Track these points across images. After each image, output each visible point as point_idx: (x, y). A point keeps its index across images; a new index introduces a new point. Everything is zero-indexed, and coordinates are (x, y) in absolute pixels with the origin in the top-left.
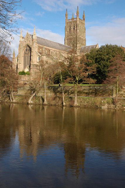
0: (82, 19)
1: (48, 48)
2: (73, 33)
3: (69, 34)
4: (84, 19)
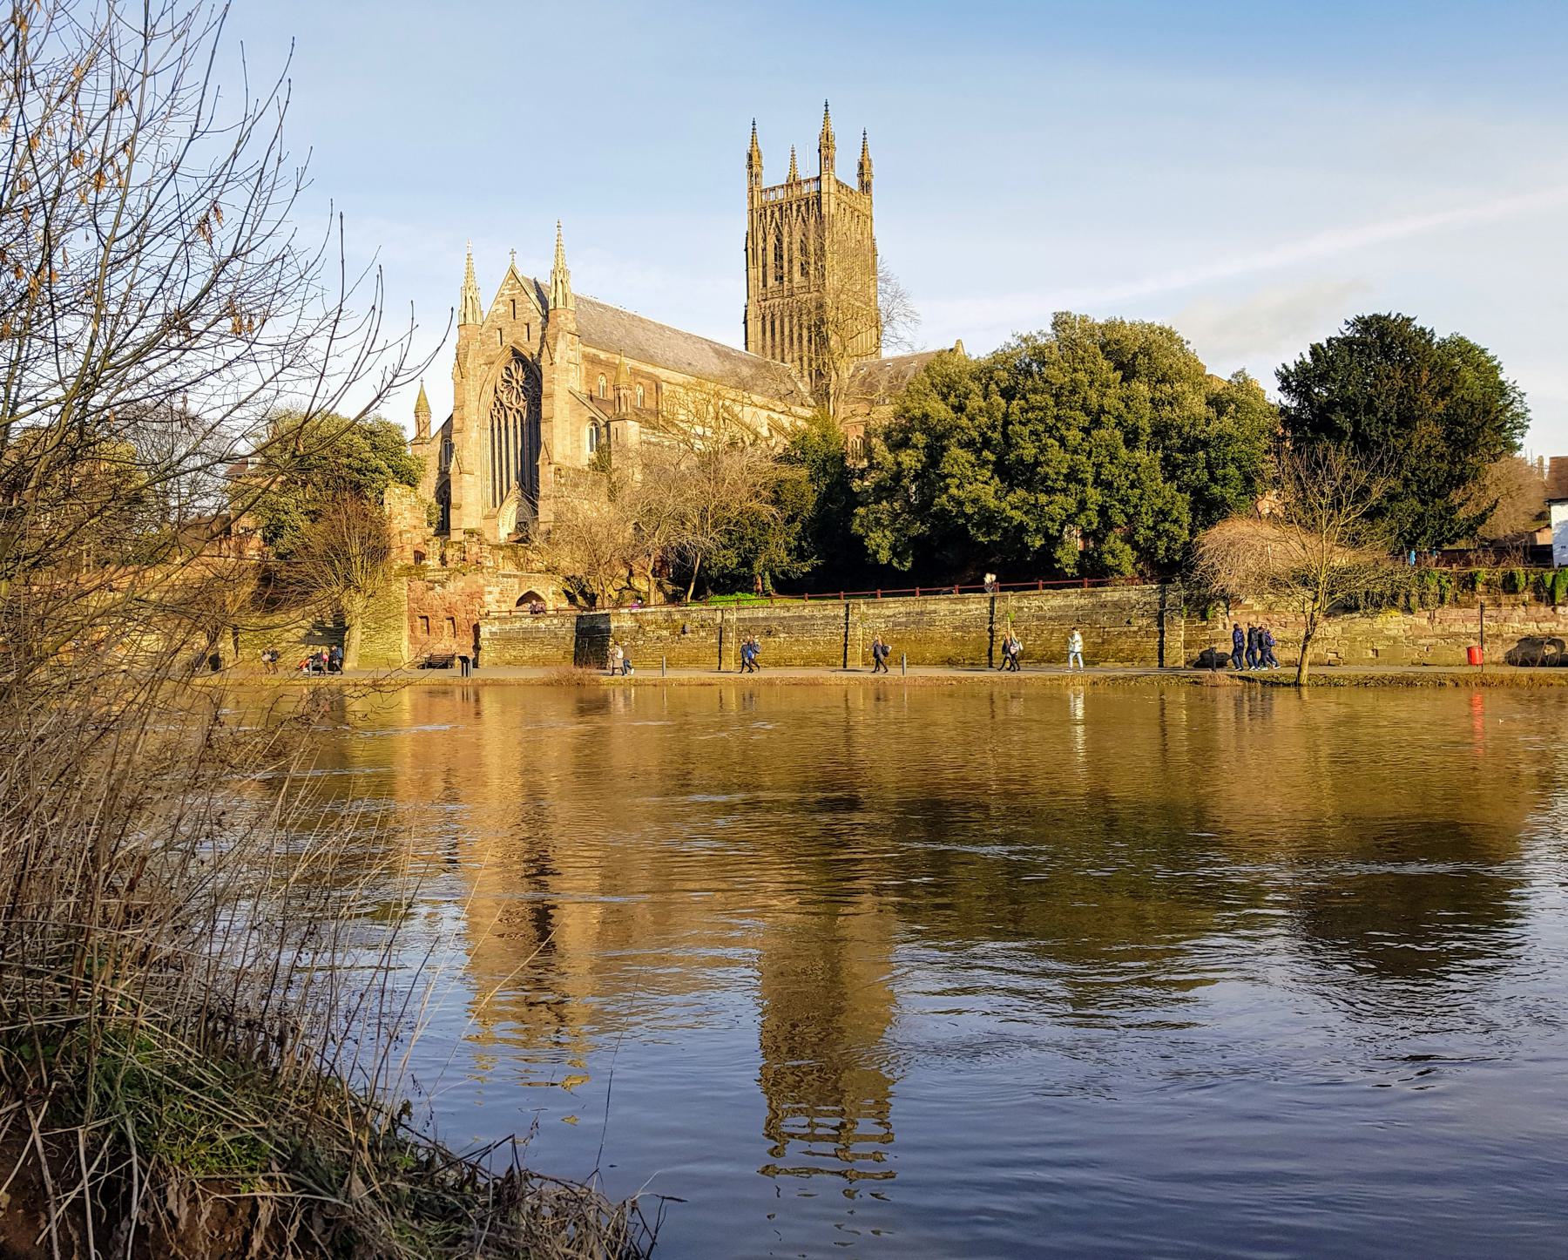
0: (854, 184)
1: (649, 369)
2: (797, 276)
3: (771, 282)
4: (865, 187)
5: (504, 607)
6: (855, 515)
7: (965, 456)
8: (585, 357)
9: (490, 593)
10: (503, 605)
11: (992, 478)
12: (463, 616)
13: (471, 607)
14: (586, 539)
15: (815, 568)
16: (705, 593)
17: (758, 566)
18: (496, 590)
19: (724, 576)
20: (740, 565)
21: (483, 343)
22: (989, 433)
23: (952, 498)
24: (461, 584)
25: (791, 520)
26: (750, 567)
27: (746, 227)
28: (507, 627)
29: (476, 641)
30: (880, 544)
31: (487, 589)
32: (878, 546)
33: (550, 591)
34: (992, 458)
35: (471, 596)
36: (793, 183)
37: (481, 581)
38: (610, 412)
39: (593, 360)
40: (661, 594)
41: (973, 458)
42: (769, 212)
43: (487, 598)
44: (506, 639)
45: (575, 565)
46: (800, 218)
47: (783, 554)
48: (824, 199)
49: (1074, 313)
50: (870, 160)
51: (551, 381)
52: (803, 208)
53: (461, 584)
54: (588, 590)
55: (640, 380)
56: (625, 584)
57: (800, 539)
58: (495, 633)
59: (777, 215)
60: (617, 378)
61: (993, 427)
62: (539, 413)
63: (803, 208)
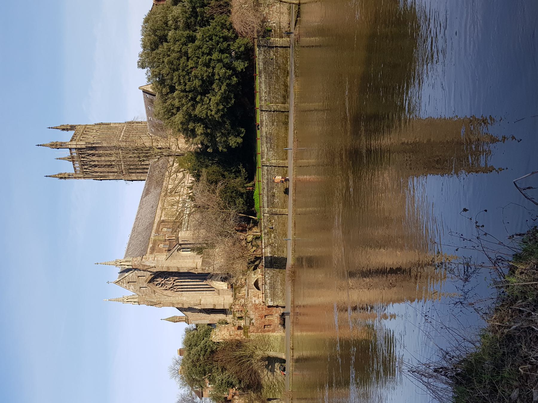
5: (261, 295)
6: (222, 150)
7: (198, 108)
8: (151, 253)
9: (255, 301)
10: (260, 296)
11: (208, 97)
12: (264, 312)
13: (261, 309)
14: (231, 259)
15: (244, 167)
16: (253, 211)
17: (242, 190)
18: (254, 299)
19: (247, 203)
20: (242, 197)
21: (146, 295)
22: (189, 98)
23: (216, 113)
24: (251, 312)
25: (223, 176)
26: (243, 193)
27: (91, 180)
28: (269, 295)
29: (274, 307)
30: (234, 141)
31: (253, 302)
32: (235, 142)
33: (254, 276)
34: (199, 97)
35: (256, 308)
36: (72, 159)
37: (250, 305)
38: (175, 243)
39: (153, 250)
40: (254, 229)
41: (200, 105)
42: (85, 170)
43: (257, 302)
44: (274, 296)
45: (240, 266)
46: (87, 157)
47: (237, 180)
48: (79, 147)
49: (138, 60)
50: (61, 126)
51: (162, 267)
52: (83, 156)
53: (251, 312)
54: (252, 260)
55: (160, 230)
56: (250, 244)
57: (231, 172)
58: (271, 300)
59: (86, 167)
60: (159, 240)
61: (187, 96)
62: (175, 272)
63: (83, 156)
